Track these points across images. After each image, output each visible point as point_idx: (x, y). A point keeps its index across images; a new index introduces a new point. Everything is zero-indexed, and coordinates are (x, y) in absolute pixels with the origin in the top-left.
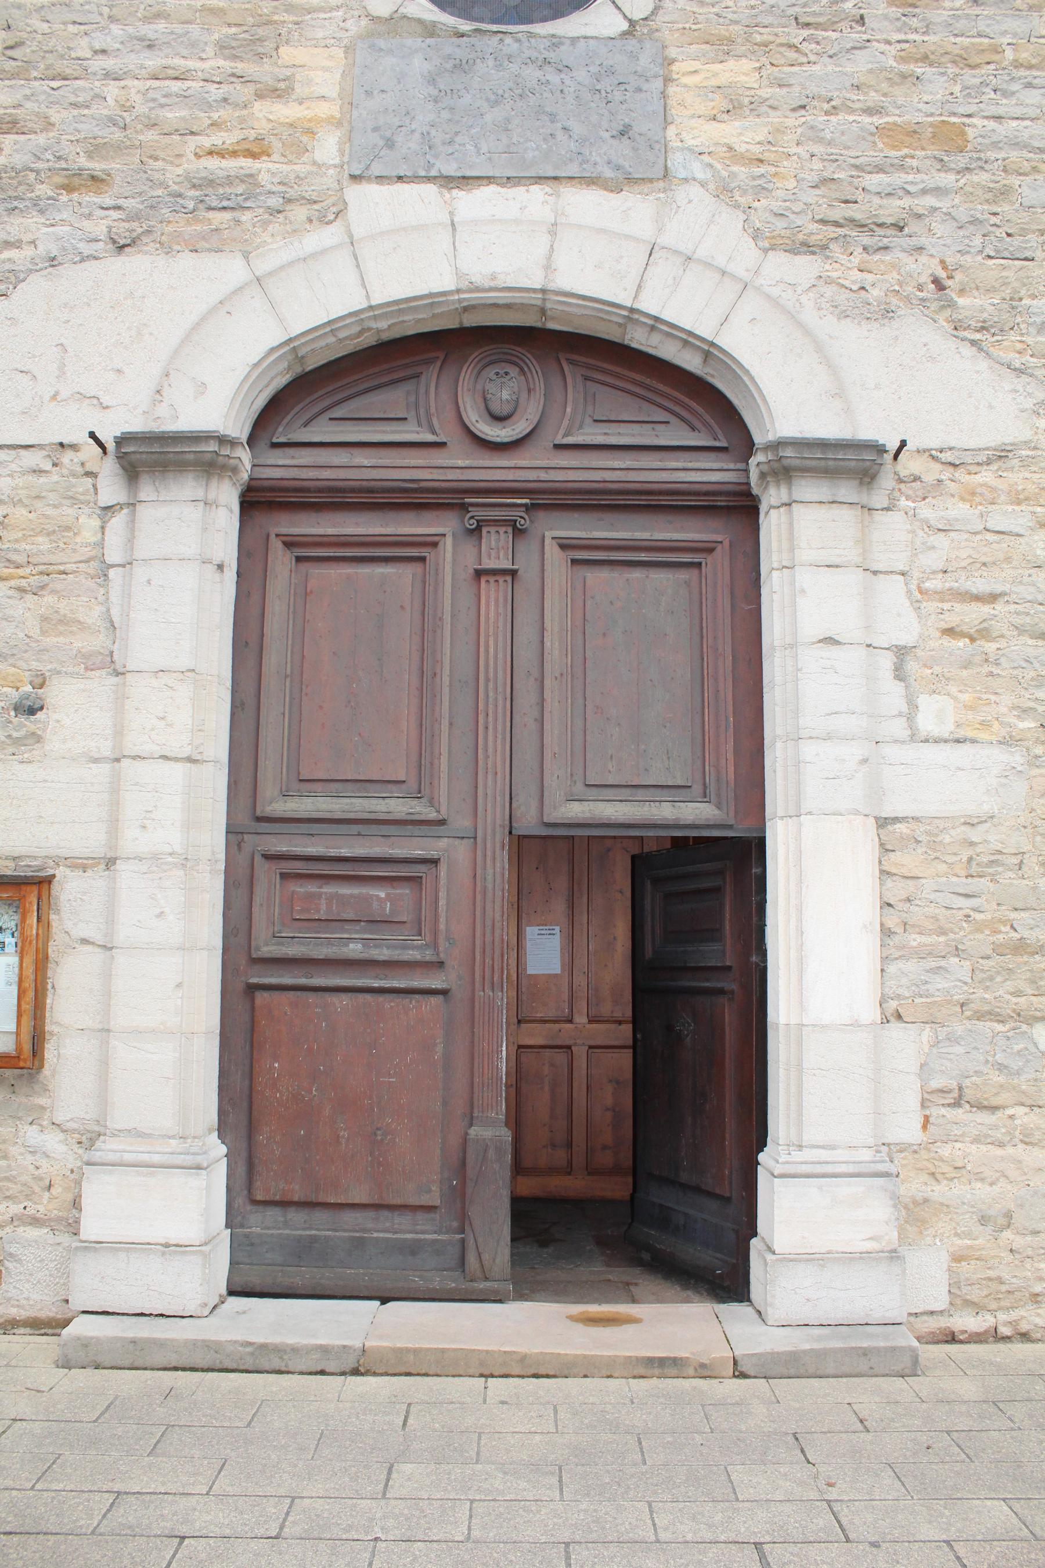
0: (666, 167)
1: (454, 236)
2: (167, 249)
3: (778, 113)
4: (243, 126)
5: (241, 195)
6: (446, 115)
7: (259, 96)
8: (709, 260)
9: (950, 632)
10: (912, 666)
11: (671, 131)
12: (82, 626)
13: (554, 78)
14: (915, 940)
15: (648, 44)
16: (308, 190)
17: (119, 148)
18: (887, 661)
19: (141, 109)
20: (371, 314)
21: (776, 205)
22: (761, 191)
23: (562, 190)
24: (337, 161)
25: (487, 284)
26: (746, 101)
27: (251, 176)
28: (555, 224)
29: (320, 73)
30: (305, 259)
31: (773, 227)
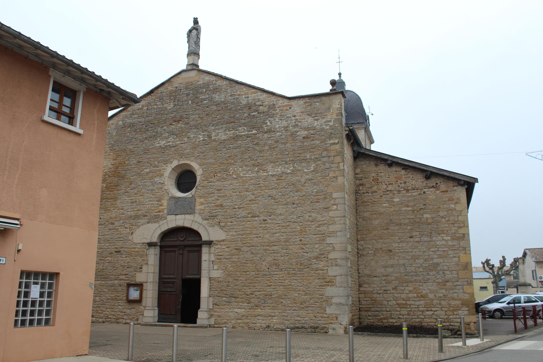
2: (152, 223)
9: (218, 259)
12: (145, 260)
14: (213, 289)
17: (148, 212)
18: (211, 262)
19: (150, 208)
22: (203, 214)
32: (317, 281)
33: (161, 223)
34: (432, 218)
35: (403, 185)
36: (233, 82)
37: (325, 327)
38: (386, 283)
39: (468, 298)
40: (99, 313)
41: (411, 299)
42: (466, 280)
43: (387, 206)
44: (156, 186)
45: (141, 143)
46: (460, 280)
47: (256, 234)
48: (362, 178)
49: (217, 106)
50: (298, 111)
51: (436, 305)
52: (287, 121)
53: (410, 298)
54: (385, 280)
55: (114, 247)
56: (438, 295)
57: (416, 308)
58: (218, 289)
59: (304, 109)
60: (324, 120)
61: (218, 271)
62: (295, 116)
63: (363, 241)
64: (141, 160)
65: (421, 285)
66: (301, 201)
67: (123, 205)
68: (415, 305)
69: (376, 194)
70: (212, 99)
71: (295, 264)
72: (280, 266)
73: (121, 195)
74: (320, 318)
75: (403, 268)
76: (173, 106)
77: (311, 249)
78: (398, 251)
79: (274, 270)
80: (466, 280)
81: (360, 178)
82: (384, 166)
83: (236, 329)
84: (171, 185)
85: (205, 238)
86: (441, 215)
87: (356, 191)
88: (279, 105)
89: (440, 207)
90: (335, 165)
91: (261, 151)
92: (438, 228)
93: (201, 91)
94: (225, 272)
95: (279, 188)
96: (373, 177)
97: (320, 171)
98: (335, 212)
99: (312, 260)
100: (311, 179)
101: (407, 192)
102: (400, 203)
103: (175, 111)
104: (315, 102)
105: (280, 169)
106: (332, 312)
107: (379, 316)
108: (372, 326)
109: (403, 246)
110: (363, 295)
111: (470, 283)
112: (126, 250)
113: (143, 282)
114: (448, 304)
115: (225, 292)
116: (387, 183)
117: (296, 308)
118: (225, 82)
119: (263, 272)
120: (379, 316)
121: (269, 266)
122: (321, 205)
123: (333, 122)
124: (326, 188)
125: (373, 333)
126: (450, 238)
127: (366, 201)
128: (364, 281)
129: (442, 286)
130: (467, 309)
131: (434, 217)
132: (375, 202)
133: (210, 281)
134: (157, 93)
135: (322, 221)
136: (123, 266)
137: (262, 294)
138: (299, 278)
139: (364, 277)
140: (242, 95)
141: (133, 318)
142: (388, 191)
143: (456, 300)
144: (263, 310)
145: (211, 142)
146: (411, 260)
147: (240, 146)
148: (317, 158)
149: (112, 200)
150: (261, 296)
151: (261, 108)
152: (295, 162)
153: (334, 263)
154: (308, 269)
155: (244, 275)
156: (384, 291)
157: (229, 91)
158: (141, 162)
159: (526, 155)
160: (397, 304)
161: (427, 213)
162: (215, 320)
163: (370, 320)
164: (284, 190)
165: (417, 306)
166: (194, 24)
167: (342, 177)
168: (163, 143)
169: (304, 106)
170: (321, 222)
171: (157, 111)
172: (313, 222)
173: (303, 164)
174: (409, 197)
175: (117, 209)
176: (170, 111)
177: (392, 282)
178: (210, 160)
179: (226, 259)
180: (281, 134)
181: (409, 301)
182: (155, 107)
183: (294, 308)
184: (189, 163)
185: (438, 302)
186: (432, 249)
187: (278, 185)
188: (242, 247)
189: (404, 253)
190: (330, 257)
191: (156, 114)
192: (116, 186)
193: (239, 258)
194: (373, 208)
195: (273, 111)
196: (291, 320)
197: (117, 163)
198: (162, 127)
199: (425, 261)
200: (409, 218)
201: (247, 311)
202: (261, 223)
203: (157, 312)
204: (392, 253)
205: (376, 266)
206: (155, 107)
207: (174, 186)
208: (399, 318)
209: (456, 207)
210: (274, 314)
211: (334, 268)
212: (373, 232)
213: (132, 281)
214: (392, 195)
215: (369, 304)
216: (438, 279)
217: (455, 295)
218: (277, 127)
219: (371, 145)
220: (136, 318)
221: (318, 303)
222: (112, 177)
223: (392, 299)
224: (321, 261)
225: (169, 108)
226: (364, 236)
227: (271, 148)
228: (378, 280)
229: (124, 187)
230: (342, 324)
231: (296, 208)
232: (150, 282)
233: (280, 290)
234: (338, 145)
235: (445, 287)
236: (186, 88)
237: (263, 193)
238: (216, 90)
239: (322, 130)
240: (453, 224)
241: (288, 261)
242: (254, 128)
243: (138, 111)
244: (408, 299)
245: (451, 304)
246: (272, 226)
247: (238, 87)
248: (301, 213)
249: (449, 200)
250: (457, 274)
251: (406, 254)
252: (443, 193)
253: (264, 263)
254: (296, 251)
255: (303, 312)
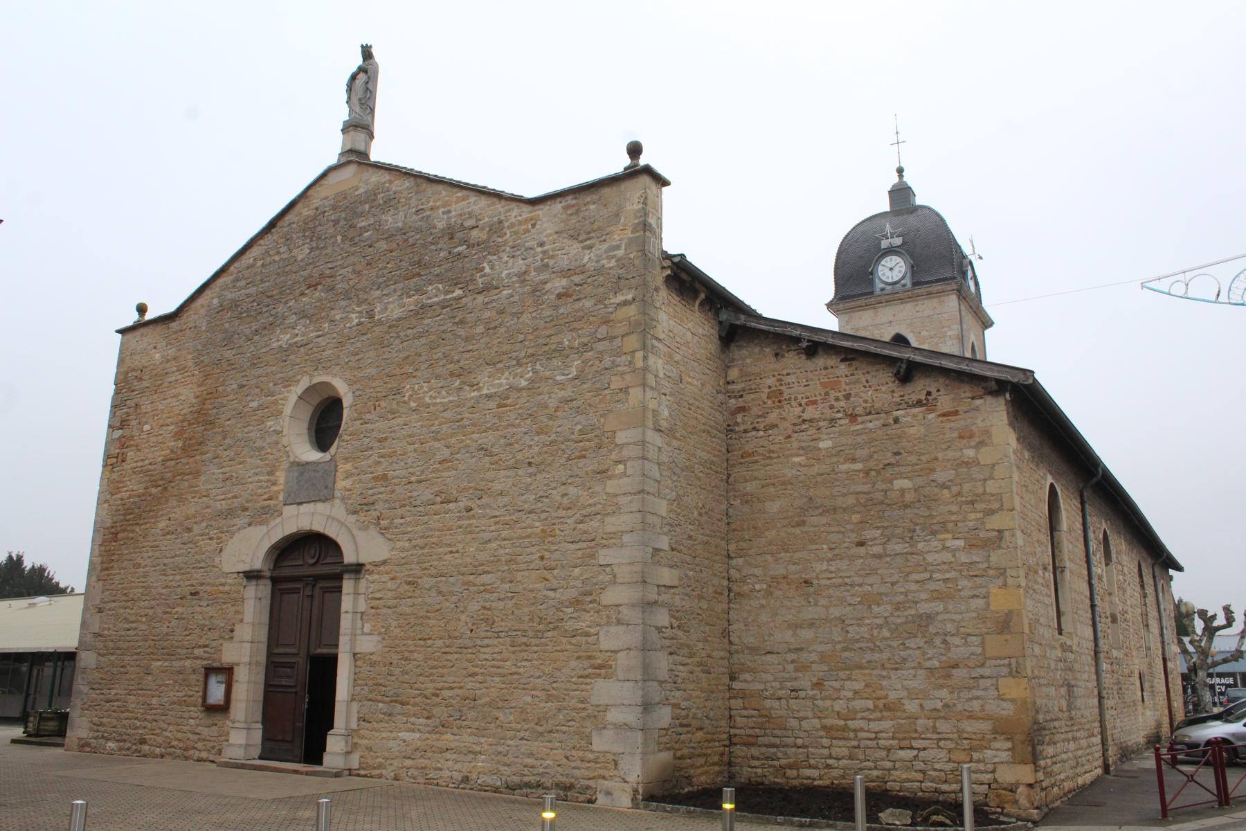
2: (256, 525)
10: (364, 616)
14: (360, 682)
18: (359, 615)
22: (349, 499)
32: (573, 663)
33: (272, 523)
34: (915, 490)
35: (842, 403)
36: (421, 180)
37: (588, 788)
38: (796, 670)
39: (1011, 713)
40: (156, 735)
41: (859, 715)
42: (1006, 662)
43: (803, 463)
44: (268, 440)
45: (248, 343)
46: (988, 663)
47: (450, 545)
48: (744, 390)
49: (389, 240)
50: (549, 231)
51: (923, 733)
52: (524, 259)
53: (855, 711)
54: (792, 662)
55: (188, 583)
56: (929, 705)
57: (871, 739)
58: (370, 683)
59: (563, 224)
60: (605, 246)
61: (371, 636)
62: (542, 245)
63: (741, 557)
64: (244, 383)
65: (885, 677)
66: (546, 455)
67: (208, 487)
68: (868, 731)
69: (775, 431)
70: (380, 226)
71: (526, 618)
72: (496, 624)
73: (208, 463)
74: (578, 763)
75: (839, 630)
76: (308, 251)
77: (564, 579)
78: (828, 582)
79: (483, 634)
80: (1006, 662)
81: (739, 392)
82: (797, 357)
83: (400, 782)
84: (298, 435)
85: (349, 557)
86: (940, 481)
87: (729, 425)
88: (510, 221)
89: (936, 459)
90: (624, 358)
91: (467, 339)
92: (931, 516)
93: (360, 209)
94: (384, 639)
95: (501, 428)
96: (770, 387)
97: (590, 377)
98: (621, 480)
99: (564, 609)
100: (569, 399)
101: (851, 422)
102: (834, 452)
103: (311, 264)
104: (588, 203)
105: (506, 379)
106: (605, 748)
107: (778, 759)
108: (761, 787)
109: (839, 570)
110: (740, 701)
111: (1017, 671)
112: (208, 588)
113: (234, 664)
114: (955, 731)
115: (384, 689)
116: (803, 402)
117: (527, 734)
118: (408, 183)
119: (460, 641)
120: (778, 759)
121: (473, 624)
122: (590, 464)
123: (625, 249)
124: (602, 420)
125: (699, 809)
126: (963, 544)
127: (750, 451)
128: (743, 664)
129: (940, 677)
130: (1009, 745)
131: (919, 487)
132: (773, 452)
133: (356, 660)
134: (282, 227)
135: (590, 505)
136: (202, 627)
137: (457, 696)
138: (535, 656)
139: (743, 652)
140: (438, 208)
141: (213, 747)
142: (804, 421)
143: (978, 718)
144: (458, 737)
145: (372, 327)
146: (860, 607)
147: (427, 331)
148: (585, 345)
149: (191, 476)
150: (454, 702)
151: (475, 233)
152: (537, 360)
153: (614, 617)
154: (555, 633)
155: (422, 646)
156: (792, 691)
157: (413, 202)
158: (244, 386)
159: (1143, 287)
160: (824, 728)
161: (901, 476)
162: (362, 757)
163: (754, 770)
164: (511, 430)
165: (874, 735)
166: (364, 61)
167: (638, 388)
168: (285, 339)
169: (564, 216)
170: (589, 509)
171: (279, 268)
172: (569, 508)
173: (556, 363)
174: (857, 435)
175: (198, 495)
176: (301, 264)
177: (810, 667)
178: (368, 371)
179: (389, 608)
180: (511, 291)
181: (855, 719)
182: (277, 258)
183: (522, 734)
184: (329, 381)
185: (931, 723)
186: (915, 577)
187: (500, 418)
188: (421, 578)
189: (843, 588)
190: (604, 603)
191: (278, 274)
192: (200, 444)
193: (414, 605)
194: (768, 468)
195: (499, 237)
196: (515, 763)
197: (205, 392)
198: (286, 302)
199: (897, 609)
200: (857, 493)
201: (424, 738)
202: (461, 517)
203: (257, 736)
204: (812, 590)
205: (772, 625)
206: (277, 258)
207: (306, 437)
208: (828, 766)
209: (979, 457)
210: (478, 749)
211: (614, 629)
212: (767, 534)
213: (214, 660)
214: (814, 431)
215: (753, 725)
216: (930, 659)
217: (976, 705)
218: (503, 275)
219: (987, 332)
220: (217, 748)
221: (574, 720)
222: (194, 424)
223: (810, 714)
224: (585, 610)
225: (300, 258)
226: (744, 545)
227: (490, 329)
228: (776, 662)
229: (212, 444)
230: (628, 780)
231: (535, 475)
232: (245, 664)
233: (494, 687)
234: (633, 307)
235: (949, 682)
236: (334, 208)
237: (468, 442)
238: (390, 203)
239: (600, 271)
240: (972, 502)
241: (513, 612)
242: (456, 284)
243: (248, 271)
244: (851, 715)
245: (963, 731)
246: (483, 522)
247: (431, 189)
248: (545, 488)
249: (961, 437)
250: (983, 644)
251: (848, 591)
252: (945, 418)
253: (463, 617)
254: (531, 587)
255: (541, 744)
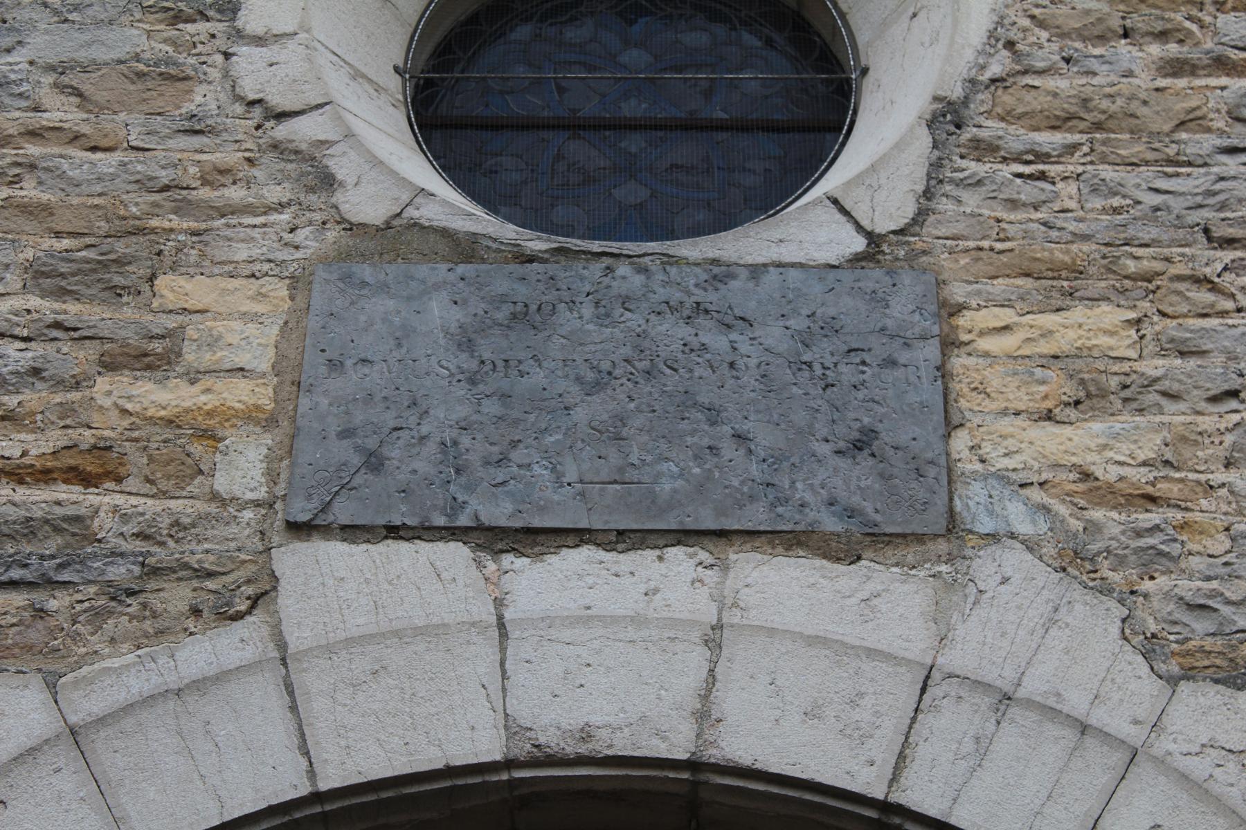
0: (951, 512)
1: (503, 649)
3: (1182, 406)
4: (68, 422)
5: (53, 557)
6: (492, 408)
7: (109, 365)
8: (1051, 702)
11: (960, 442)
13: (718, 341)
15: (906, 278)
16: (198, 553)
20: (318, 809)
21: (1187, 587)
23: (733, 557)
24: (262, 493)
25: (572, 749)
26: (1114, 382)
27: (77, 519)
28: (718, 627)
29: (237, 325)
30: (178, 692)
31: (1186, 633)
